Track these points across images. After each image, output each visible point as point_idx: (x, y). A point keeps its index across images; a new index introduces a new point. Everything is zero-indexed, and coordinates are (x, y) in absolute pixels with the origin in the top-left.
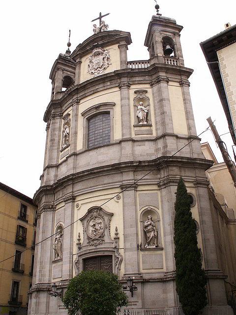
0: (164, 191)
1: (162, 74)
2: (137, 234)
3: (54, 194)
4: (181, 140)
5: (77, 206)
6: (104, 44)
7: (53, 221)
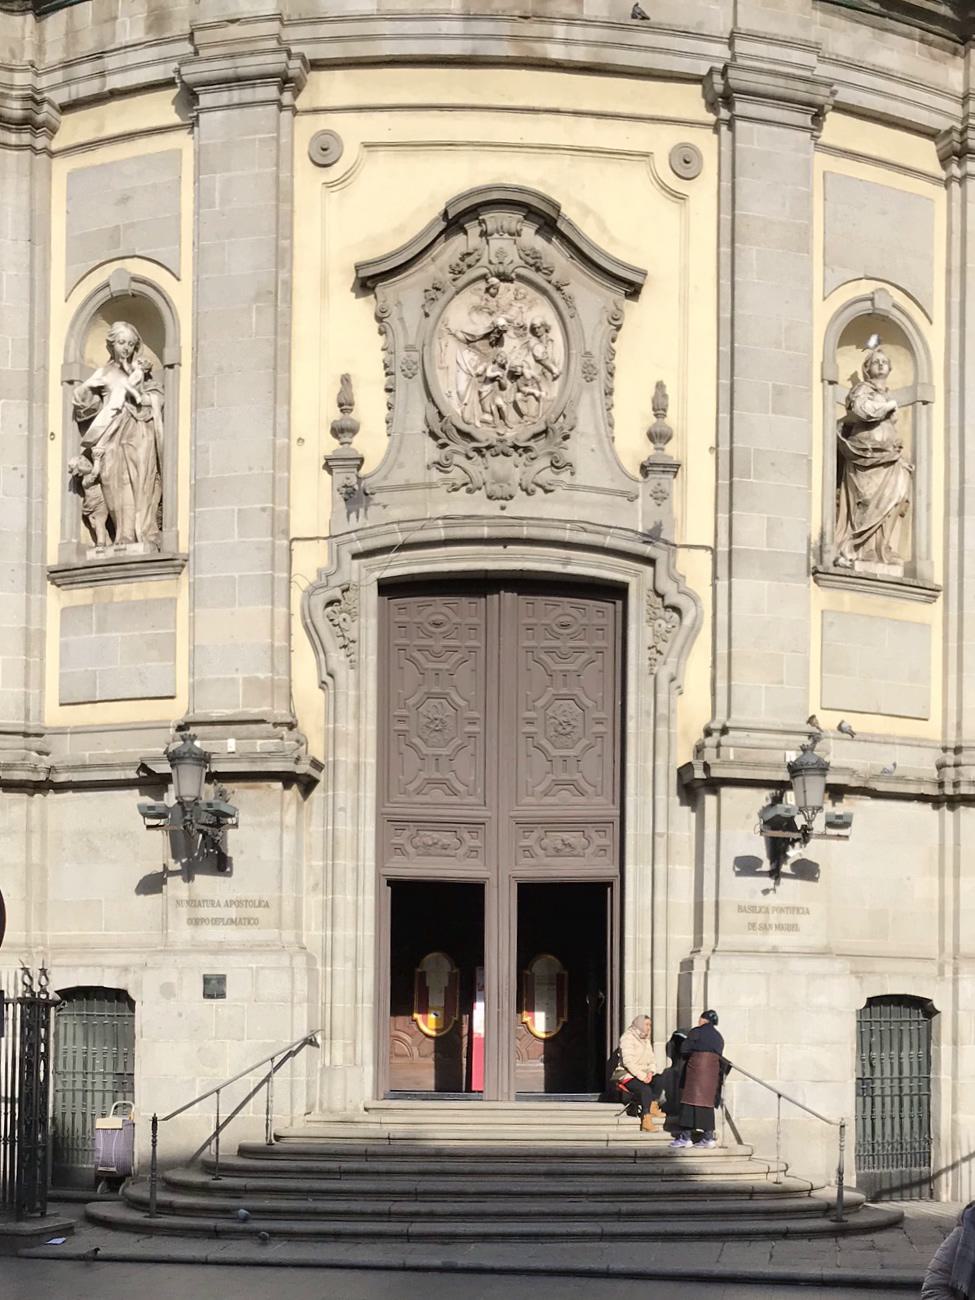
5: (324, 154)
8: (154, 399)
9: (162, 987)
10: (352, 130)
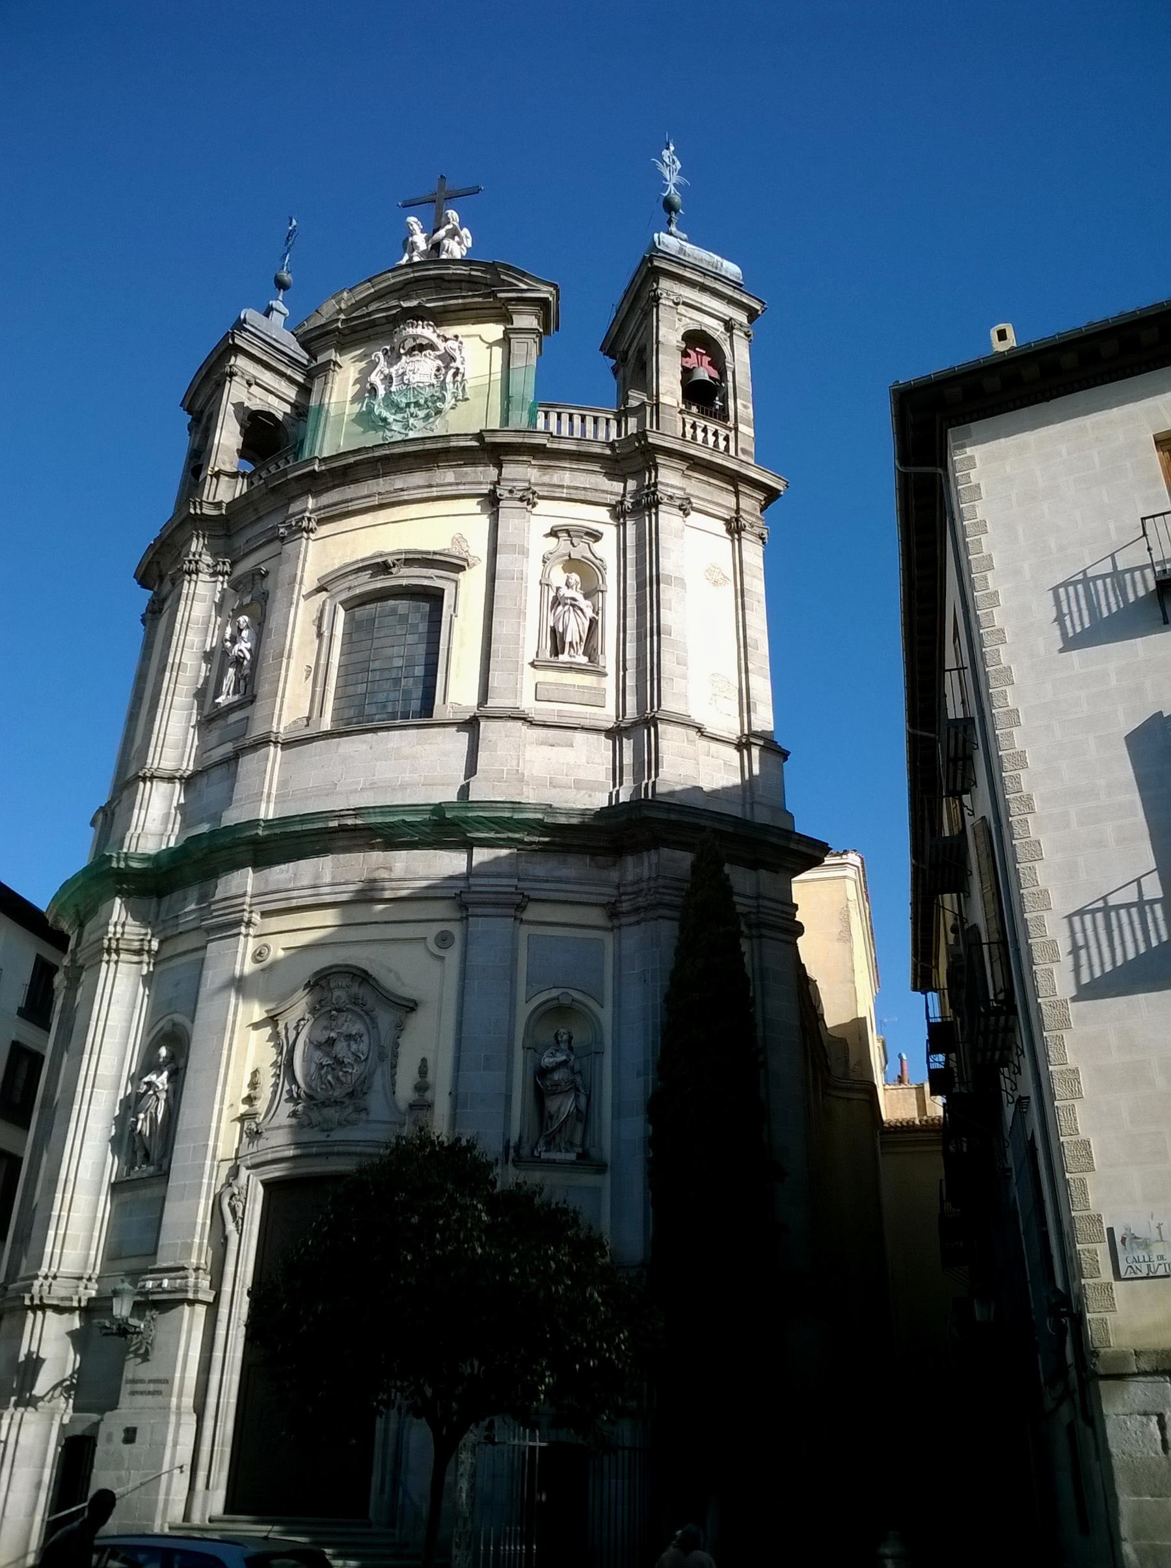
0: (633, 937)
1: (670, 478)
2: (508, 1098)
4: (715, 746)
6: (445, 310)
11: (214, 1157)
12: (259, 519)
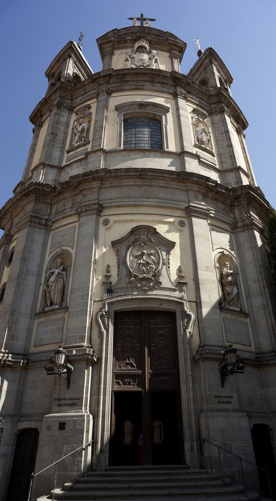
3: (51, 205)
5: (106, 222)
7: (45, 245)
8: (64, 273)
9: (47, 427)
10: (112, 219)
11: (91, 300)
12: (86, 93)
